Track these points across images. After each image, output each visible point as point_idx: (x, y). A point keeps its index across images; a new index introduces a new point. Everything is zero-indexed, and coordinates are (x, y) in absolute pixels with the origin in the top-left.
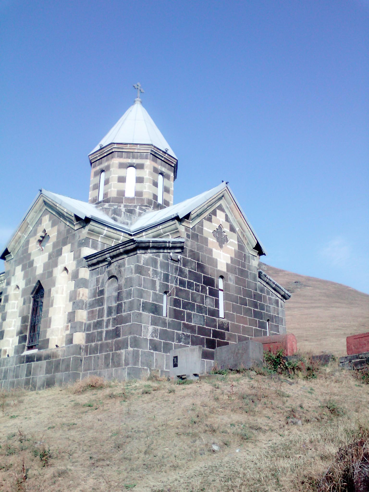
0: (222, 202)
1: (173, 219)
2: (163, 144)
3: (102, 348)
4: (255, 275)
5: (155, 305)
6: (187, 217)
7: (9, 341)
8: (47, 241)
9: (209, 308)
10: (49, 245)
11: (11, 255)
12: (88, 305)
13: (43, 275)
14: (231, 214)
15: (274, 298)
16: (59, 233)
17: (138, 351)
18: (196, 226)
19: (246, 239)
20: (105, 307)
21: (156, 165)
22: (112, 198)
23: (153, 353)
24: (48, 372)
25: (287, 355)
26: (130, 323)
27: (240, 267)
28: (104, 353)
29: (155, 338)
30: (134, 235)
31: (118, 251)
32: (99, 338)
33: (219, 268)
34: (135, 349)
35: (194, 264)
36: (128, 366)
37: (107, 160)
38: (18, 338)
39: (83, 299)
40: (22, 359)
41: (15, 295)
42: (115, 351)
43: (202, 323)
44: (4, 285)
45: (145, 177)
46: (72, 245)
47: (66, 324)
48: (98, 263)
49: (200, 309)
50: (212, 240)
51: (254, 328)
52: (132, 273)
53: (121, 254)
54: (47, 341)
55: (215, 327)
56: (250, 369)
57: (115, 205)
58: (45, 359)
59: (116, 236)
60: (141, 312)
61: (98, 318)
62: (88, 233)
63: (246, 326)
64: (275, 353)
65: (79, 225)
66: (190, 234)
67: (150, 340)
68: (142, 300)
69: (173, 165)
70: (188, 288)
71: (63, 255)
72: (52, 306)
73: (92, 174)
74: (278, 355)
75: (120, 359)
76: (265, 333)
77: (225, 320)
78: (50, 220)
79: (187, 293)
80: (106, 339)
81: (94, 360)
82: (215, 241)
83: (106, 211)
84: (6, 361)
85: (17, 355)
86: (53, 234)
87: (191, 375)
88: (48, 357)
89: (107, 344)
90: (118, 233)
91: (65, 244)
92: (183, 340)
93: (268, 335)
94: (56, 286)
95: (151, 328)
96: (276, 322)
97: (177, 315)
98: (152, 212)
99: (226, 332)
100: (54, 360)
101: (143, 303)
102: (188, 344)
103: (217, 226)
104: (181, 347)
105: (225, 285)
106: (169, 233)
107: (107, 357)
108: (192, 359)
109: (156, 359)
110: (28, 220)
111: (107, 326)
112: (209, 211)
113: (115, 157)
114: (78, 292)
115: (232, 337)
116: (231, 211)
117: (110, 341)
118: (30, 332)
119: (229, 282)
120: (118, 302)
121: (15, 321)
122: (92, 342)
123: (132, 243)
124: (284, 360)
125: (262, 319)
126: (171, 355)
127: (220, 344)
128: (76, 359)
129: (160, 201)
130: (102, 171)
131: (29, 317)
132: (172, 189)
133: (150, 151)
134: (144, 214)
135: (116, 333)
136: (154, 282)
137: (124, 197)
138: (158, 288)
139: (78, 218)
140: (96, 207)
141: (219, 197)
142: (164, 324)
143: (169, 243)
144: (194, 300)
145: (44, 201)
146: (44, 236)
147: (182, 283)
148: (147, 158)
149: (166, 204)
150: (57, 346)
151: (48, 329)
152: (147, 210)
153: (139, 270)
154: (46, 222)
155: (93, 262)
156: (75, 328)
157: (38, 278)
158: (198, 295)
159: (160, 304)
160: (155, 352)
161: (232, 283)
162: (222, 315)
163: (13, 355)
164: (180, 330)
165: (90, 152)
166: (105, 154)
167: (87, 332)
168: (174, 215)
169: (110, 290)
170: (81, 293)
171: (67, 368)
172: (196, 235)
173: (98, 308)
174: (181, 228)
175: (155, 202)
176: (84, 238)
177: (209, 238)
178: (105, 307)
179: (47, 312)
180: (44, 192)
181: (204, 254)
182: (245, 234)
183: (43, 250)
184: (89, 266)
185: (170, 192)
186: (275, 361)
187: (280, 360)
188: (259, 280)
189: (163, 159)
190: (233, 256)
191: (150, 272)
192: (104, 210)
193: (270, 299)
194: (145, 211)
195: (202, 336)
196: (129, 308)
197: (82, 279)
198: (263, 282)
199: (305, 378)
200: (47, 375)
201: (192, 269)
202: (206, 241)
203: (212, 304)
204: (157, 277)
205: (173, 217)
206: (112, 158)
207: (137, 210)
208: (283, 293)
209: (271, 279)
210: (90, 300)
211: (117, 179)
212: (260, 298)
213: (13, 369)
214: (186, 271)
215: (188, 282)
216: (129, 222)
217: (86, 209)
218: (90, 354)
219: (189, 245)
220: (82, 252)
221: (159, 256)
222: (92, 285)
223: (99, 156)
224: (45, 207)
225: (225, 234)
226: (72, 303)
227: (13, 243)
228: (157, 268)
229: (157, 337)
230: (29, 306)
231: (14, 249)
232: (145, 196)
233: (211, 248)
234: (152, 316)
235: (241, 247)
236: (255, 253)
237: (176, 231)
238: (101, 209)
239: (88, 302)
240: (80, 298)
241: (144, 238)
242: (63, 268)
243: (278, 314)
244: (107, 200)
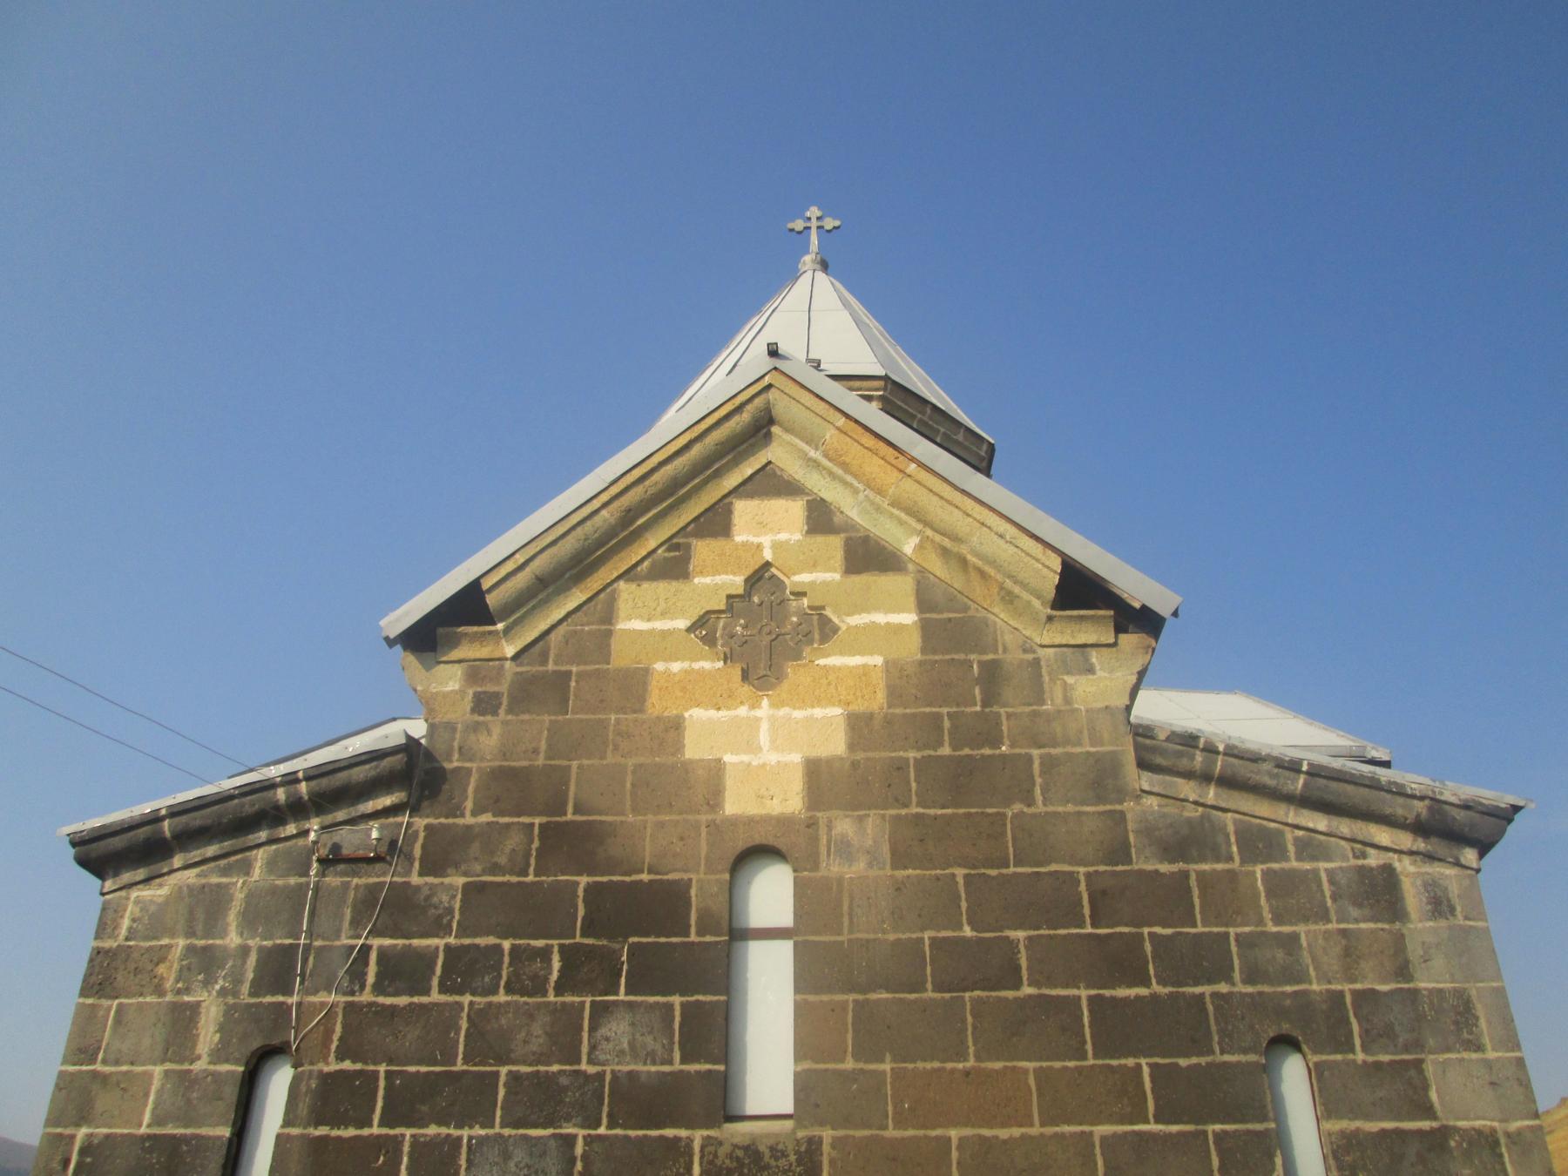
14: (846, 483)
49: (540, 1100)
77: (789, 1124)
116: (840, 472)
119: (832, 868)
125: (1199, 1044)
136: (184, 1019)
143: (291, 780)
159: (204, 1131)
182: (964, 549)
188: (1146, 781)
198: (1188, 789)
202: (634, 684)
204: (207, 983)
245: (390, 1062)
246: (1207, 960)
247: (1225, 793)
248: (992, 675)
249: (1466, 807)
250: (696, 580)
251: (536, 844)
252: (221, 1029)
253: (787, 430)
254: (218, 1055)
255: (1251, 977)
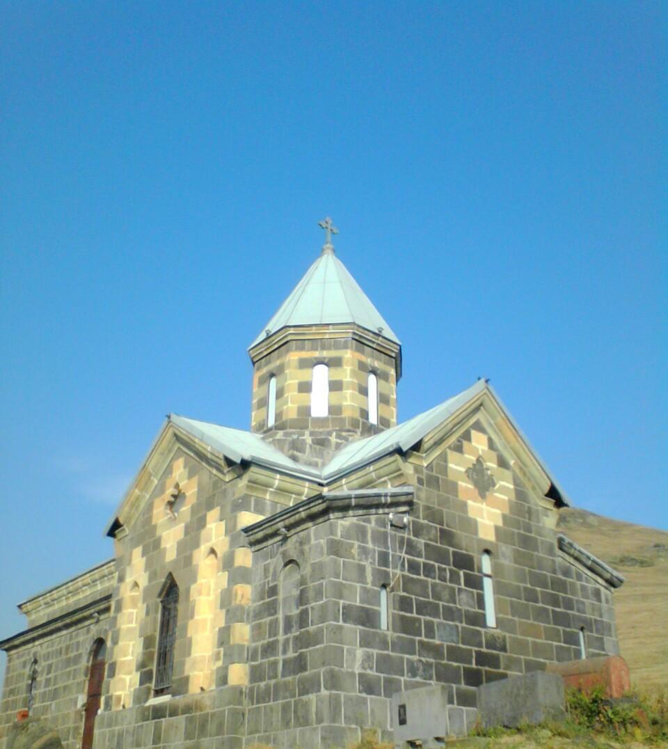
0: (480, 416)
1: (391, 454)
2: (373, 319)
3: (276, 692)
4: (551, 545)
5: (366, 611)
6: (417, 447)
7: (123, 680)
8: (182, 504)
9: (467, 612)
10: (185, 509)
11: (124, 530)
12: (251, 614)
13: (175, 562)
14: (498, 434)
15: (591, 586)
16: (201, 488)
17: (338, 696)
18: (434, 463)
19: (529, 480)
20: (280, 616)
21: (363, 359)
22: (291, 419)
23: (365, 699)
24: (188, 736)
25: (611, 696)
26: (322, 646)
27: (522, 532)
28: (280, 701)
29: (369, 672)
30: (328, 484)
31: (297, 516)
32: (271, 674)
33: (481, 535)
34: (334, 692)
35: (433, 532)
36: (322, 725)
37: (279, 357)
38: (139, 674)
39: (243, 603)
40: (146, 713)
41: (133, 599)
42: (299, 696)
43: (455, 638)
44: (114, 582)
45: (345, 380)
46: (221, 509)
47: (216, 650)
48: (266, 538)
49: (450, 614)
50: (465, 485)
51: (555, 643)
52: (322, 553)
53: (302, 521)
54: (185, 681)
55: (480, 645)
56: (540, 725)
57: (294, 433)
58: (183, 713)
59: (296, 488)
60: (341, 623)
61: (270, 637)
62: (248, 487)
63: (539, 641)
64: (589, 692)
65: (232, 472)
66: (424, 477)
67: (361, 675)
68: (341, 602)
69: (393, 355)
70: (426, 576)
71: (208, 526)
72: (192, 617)
73: (256, 381)
74: (594, 696)
75: (307, 712)
76: (578, 654)
78: (185, 467)
79: (424, 584)
80: (283, 676)
81: (266, 714)
82: (471, 486)
83: (279, 445)
84: (120, 718)
85: (137, 706)
86: (191, 491)
87: (431, 739)
88: (188, 709)
89: (286, 685)
90: (300, 482)
91: (210, 507)
92: (420, 672)
93: (584, 656)
94: (199, 582)
95: (360, 652)
96: (597, 631)
97: (406, 626)
98: (359, 440)
99: (501, 654)
100: (198, 713)
101: (344, 608)
102: (431, 678)
103: (474, 459)
104: (418, 685)
105: (496, 567)
106: (385, 478)
107: (285, 708)
108: (432, 710)
109: (372, 711)
110: (150, 467)
111: (285, 652)
112: (456, 435)
113: (292, 351)
114: (234, 592)
115: (512, 663)
117: (289, 678)
118: (159, 665)
120: (301, 608)
121: (134, 645)
122: (261, 679)
123: (320, 501)
124: (606, 707)
125: (569, 626)
126: (396, 701)
127: (491, 678)
128: (234, 713)
129: (373, 419)
130: (272, 375)
131: (155, 638)
132: (394, 396)
133: (351, 335)
134: (346, 446)
135: (299, 664)
136: (362, 569)
137: (310, 418)
138: (369, 578)
139: (229, 462)
140: (263, 439)
141: (473, 407)
142: (384, 644)
143: (386, 496)
144: (437, 596)
145: (175, 435)
146: (176, 493)
147: (413, 567)
148: (346, 347)
149: (384, 423)
150: (202, 689)
151: (187, 659)
152: (350, 438)
153: (335, 548)
154: (179, 470)
155: (257, 537)
156: (231, 655)
157: (170, 570)
158: (445, 587)
160: (369, 696)
161: (507, 562)
162: (491, 621)
163: (131, 706)
164: (414, 653)
165: (251, 345)
166: (276, 346)
167: (253, 663)
168: (392, 446)
169: (287, 587)
170: (240, 593)
171: (219, 731)
172: (435, 479)
173: (268, 619)
174: (408, 468)
175: (363, 423)
176: (242, 495)
177: (460, 483)
178: (280, 616)
179: (185, 628)
180: (174, 418)
181: (453, 511)
183: (175, 518)
184: (252, 544)
185: (392, 402)
186: (588, 706)
187: (598, 707)
189: (374, 346)
190: (507, 512)
191: (355, 551)
192: (276, 443)
193: (583, 588)
194: (346, 439)
195: (455, 664)
196: (320, 616)
197: (240, 567)
198: (567, 557)
199: (646, 739)
200: (188, 741)
201: (430, 540)
202: (454, 487)
203: (471, 602)
204: (367, 559)
205: (391, 449)
206: (288, 351)
207: (333, 439)
208: (608, 576)
209: (582, 550)
210: (255, 604)
211: (296, 387)
212: (562, 586)
213: (132, 731)
214: (418, 545)
215: (425, 564)
216: (320, 461)
217: (244, 444)
218: (258, 702)
219: (423, 497)
220: (238, 520)
221: (369, 521)
222: (258, 579)
223: (265, 350)
224: (178, 445)
225: (489, 472)
226: (224, 611)
227: (126, 509)
228: (367, 543)
229: (371, 668)
230: (155, 619)
231: (129, 519)
232: (346, 414)
233: (464, 499)
234: (361, 631)
235: (520, 494)
236: (549, 504)
237: (398, 475)
238: (270, 443)
239: (251, 609)
240: (238, 602)
241: (344, 489)
242: (208, 550)
243: (601, 616)
244: (280, 426)
245: (416, 595)
246: (569, 604)
247: (574, 561)
248: (529, 511)
249: (616, 578)
250: (466, 456)
251: (439, 534)
252: (373, 575)
253: (485, 409)
254: (374, 584)
255: (578, 611)
